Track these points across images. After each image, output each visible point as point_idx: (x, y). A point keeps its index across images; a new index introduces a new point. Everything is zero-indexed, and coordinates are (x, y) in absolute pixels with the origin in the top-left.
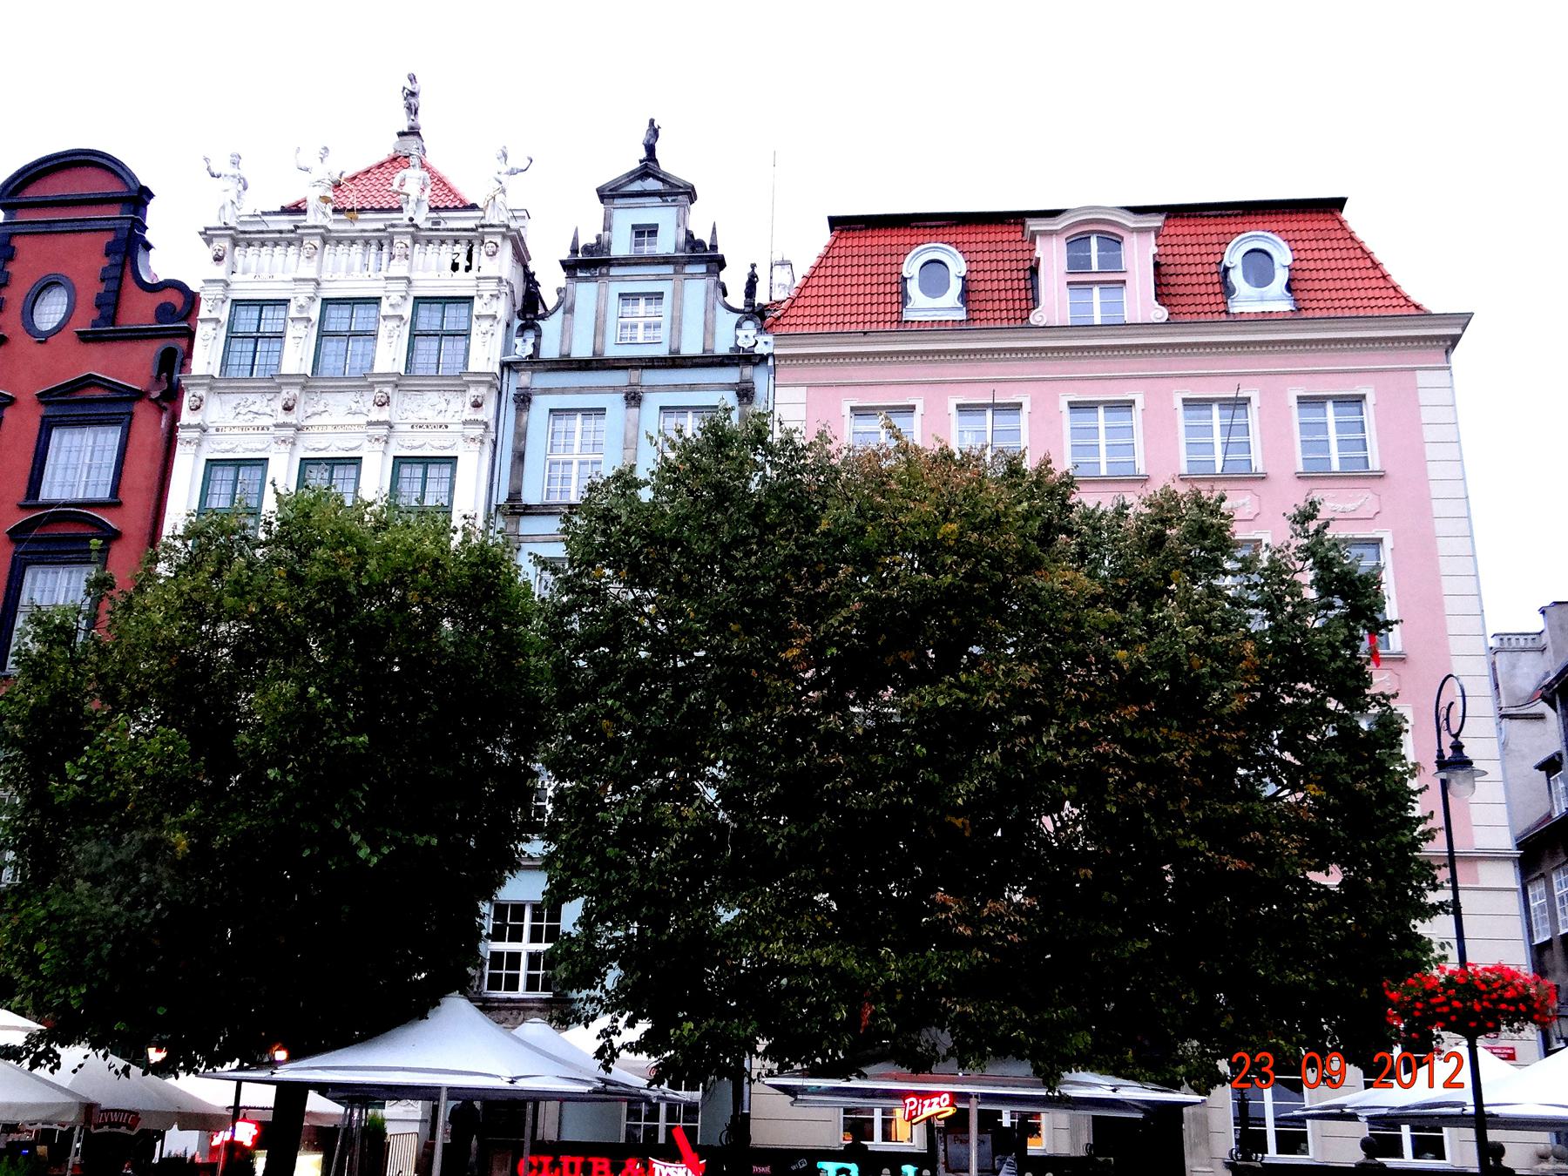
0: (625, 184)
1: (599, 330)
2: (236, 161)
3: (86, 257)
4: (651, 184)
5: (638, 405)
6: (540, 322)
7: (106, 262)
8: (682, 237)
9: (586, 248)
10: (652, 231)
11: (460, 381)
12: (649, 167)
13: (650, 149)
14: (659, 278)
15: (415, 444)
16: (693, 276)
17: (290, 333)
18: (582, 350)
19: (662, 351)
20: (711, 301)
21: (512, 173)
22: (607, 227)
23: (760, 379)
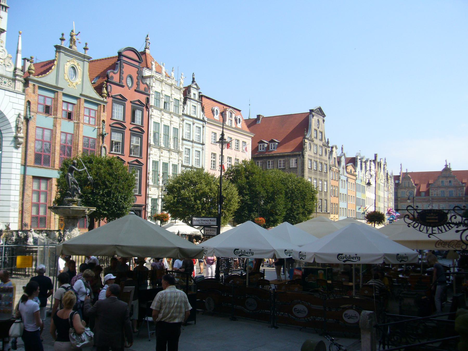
13: (193, 79)
18: (189, 114)
19: (195, 116)
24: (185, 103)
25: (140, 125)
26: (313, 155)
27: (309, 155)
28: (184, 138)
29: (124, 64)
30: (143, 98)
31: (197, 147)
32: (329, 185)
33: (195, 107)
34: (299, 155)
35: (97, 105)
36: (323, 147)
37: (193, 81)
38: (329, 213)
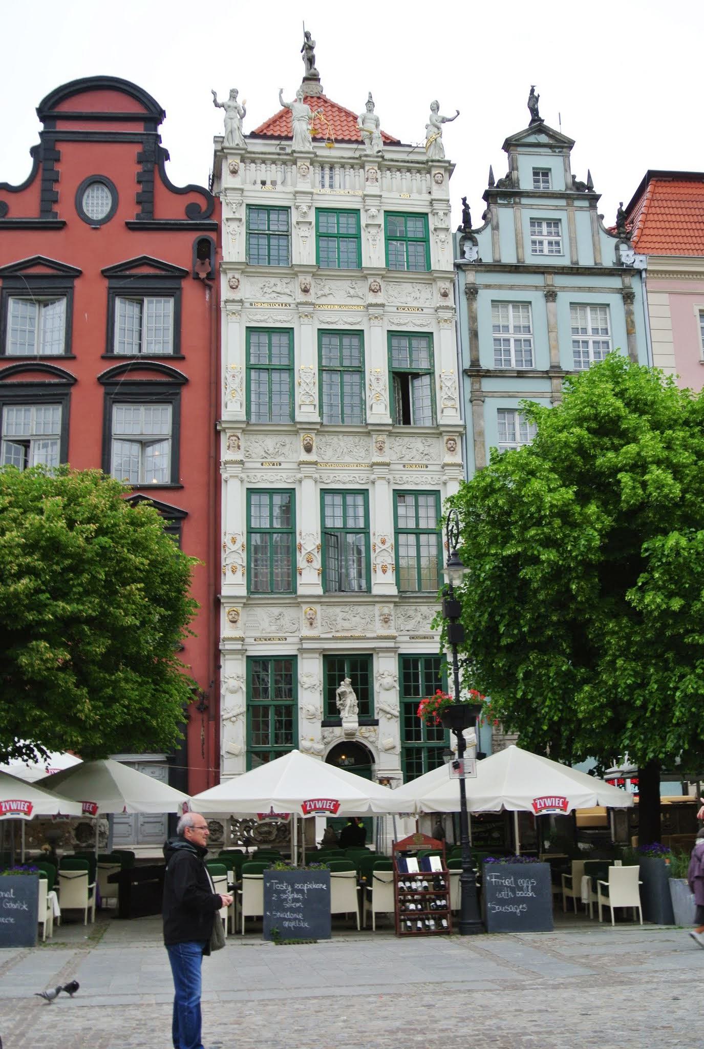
0: (525, 137)
1: (519, 244)
2: (234, 94)
3: (122, 161)
4: (543, 139)
5: (554, 300)
6: (475, 235)
7: (139, 168)
8: (570, 181)
9: (500, 181)
10: (546, 173)
12: (537, 125)
13: (534, 111)
14: (557, 208)
15: (402, 321)
16: (581, 208)
17: (294, 232)
18: (509, 258)
19: (565, 262)
20: (595, 229)
21: (444, 120)
22: (513, 167)
23: (635, 285)
28: (487, 362)
30: (177, 250)
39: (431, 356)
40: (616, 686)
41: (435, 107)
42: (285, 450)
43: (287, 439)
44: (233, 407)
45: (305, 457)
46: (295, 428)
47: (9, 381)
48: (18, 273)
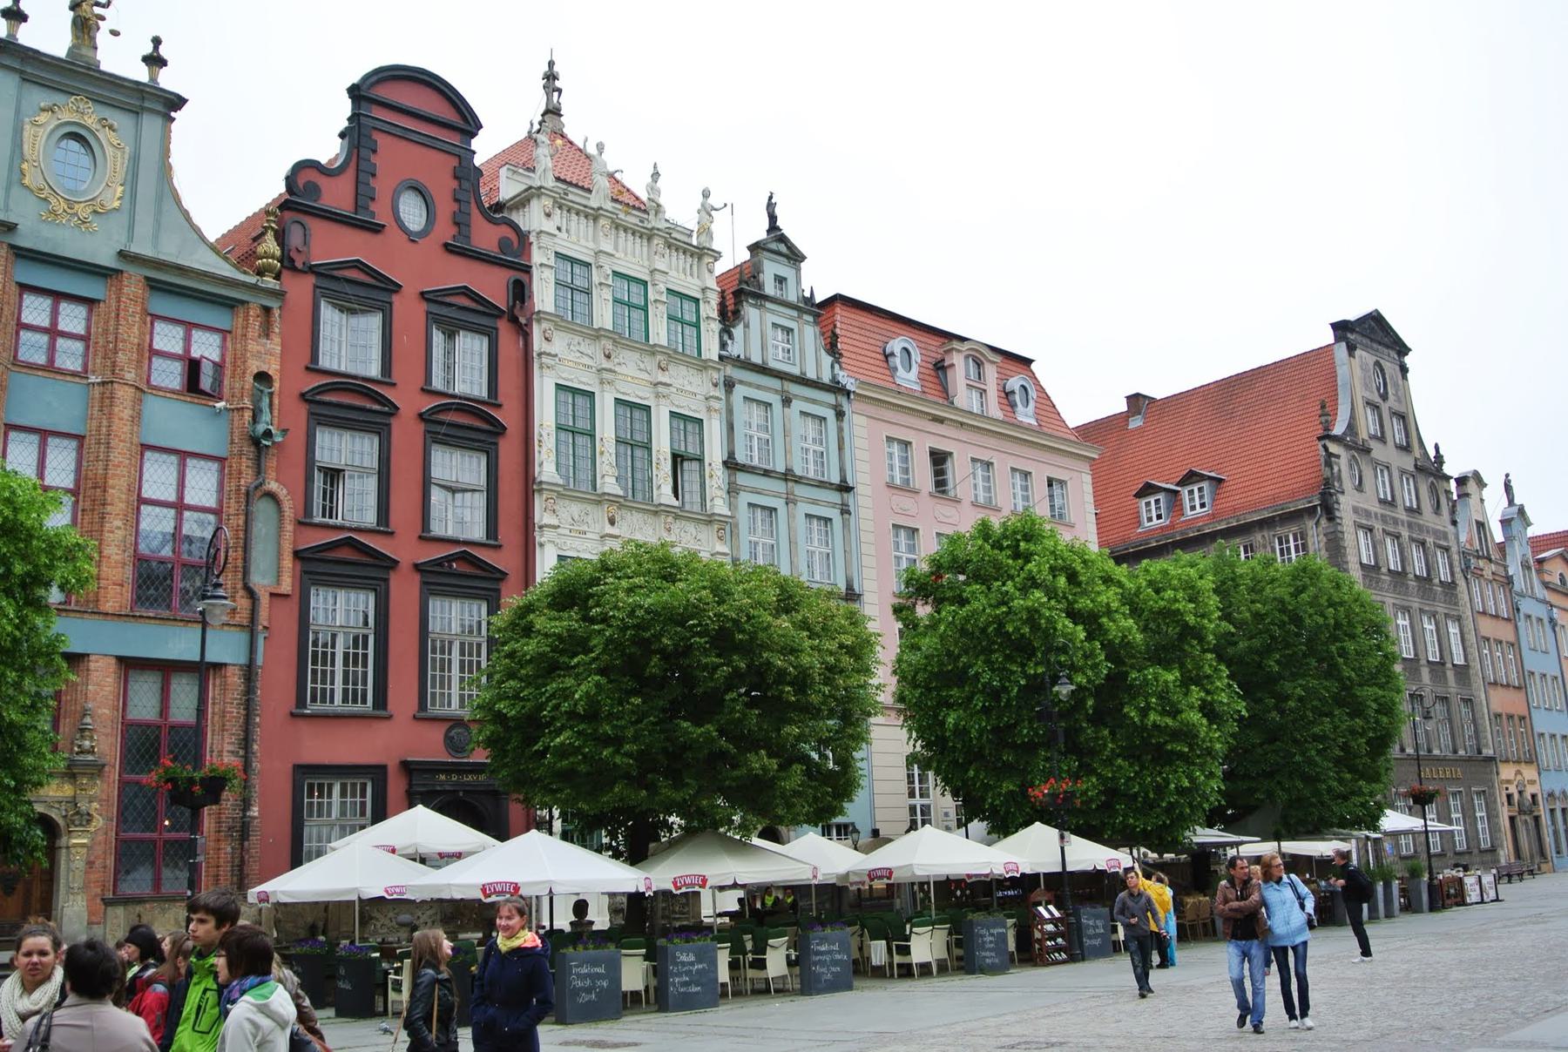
1: (763, 347)
3: (437, 171)
11: (703, 366)
13: (773, 218)
14: (792, 318)
18: (756, 359)
19: (796, 371)
24: (729, 316)
25: (485, 394)
26: (1375, 508)
27: (1356, 510)
28: (741, 458)
29: (377, 136)
30: (492, 285)
31: (815, 502)
32: (1471, 638)
33: (789, 331)
34: (1311, 511)
35: (231, 304)
36: (1420, 478)
37: (773, 227)
38: (1491, 759)
39: (702, 442)
40: (1113, 779)
41: (706, 194)
42: (589, 519)
43: (589, 508)
44: (547, 468)
45: (609, 529)
46: (601, 499)
47: (326, 398)
48: (335, 273)
